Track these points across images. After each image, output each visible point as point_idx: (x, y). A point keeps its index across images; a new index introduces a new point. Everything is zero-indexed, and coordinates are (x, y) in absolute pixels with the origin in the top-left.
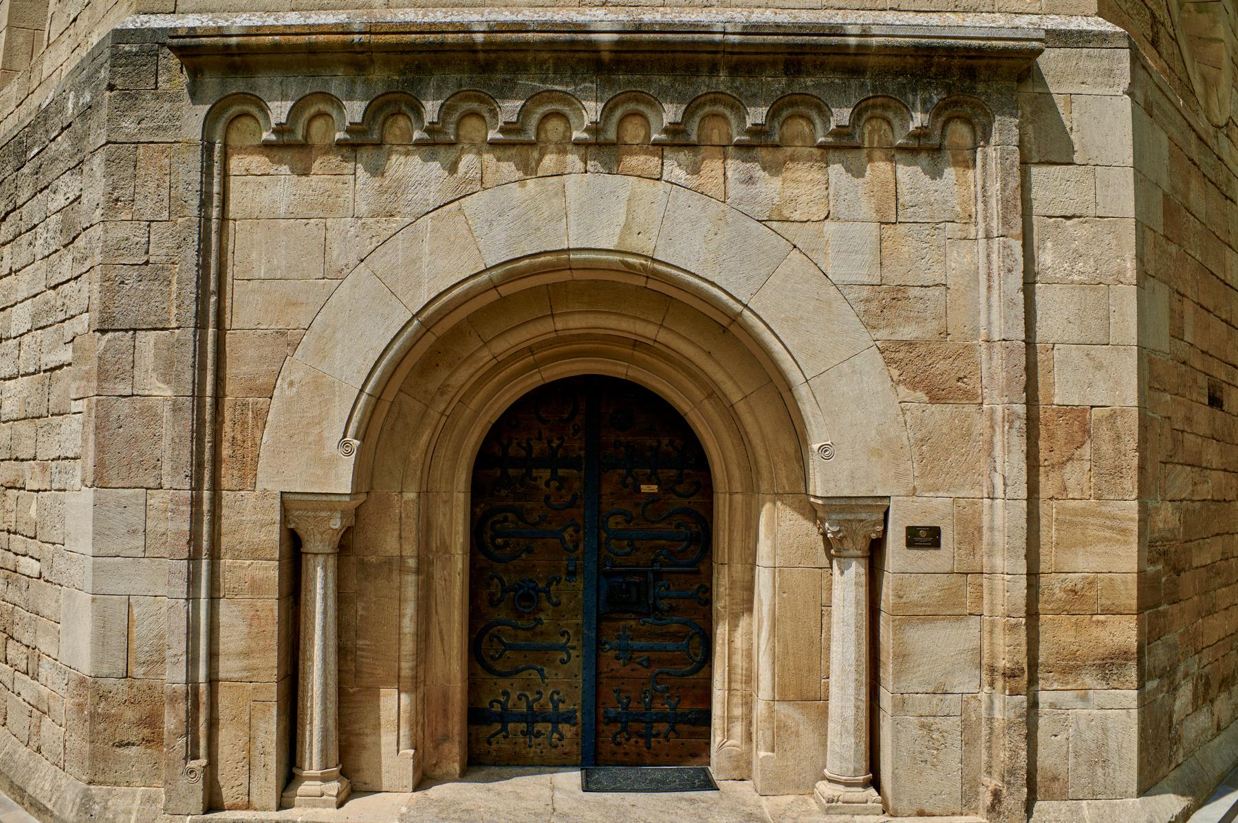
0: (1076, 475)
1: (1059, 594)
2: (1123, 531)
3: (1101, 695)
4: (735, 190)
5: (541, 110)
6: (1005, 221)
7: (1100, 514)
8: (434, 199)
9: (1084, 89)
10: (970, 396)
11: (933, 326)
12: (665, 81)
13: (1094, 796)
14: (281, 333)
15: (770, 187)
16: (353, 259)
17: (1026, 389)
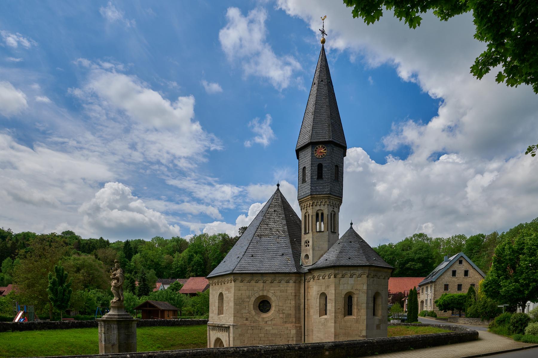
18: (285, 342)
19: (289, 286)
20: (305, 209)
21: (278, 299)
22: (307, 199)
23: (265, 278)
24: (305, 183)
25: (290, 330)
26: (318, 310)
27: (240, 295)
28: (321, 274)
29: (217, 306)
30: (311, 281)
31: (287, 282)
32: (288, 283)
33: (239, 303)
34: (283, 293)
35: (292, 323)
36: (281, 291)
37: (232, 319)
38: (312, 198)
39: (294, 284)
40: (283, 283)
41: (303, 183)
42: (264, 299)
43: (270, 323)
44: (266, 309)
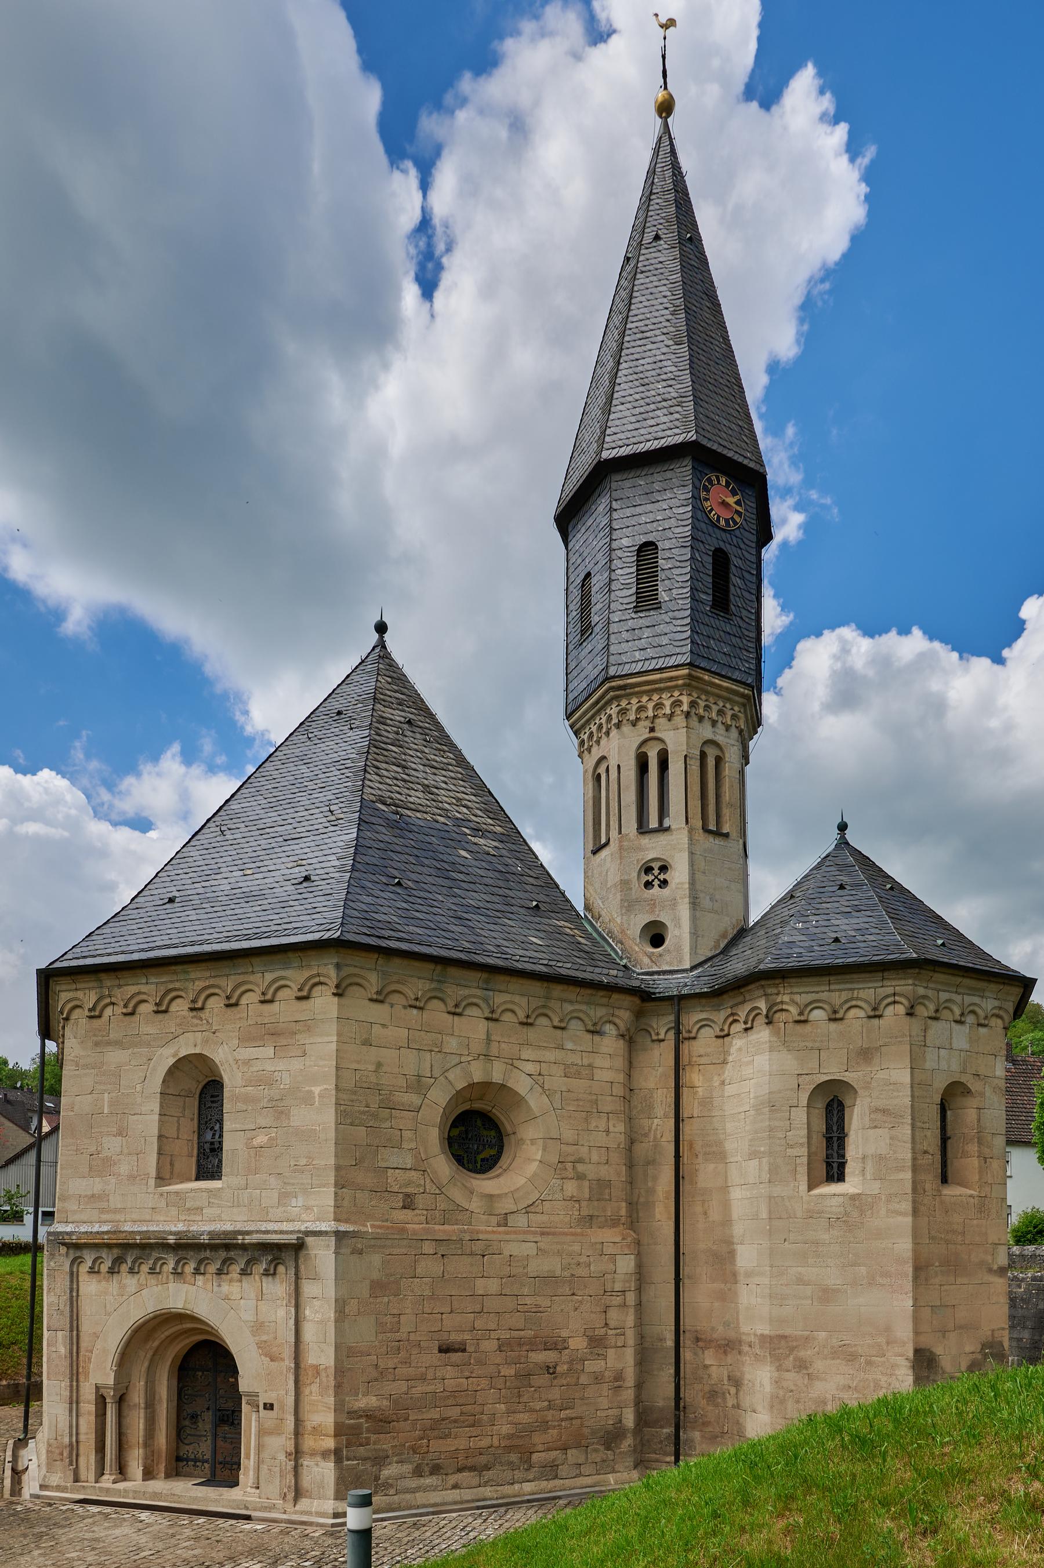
0: (315, 1388)
1: (310, 1429)
2: (329, 1408)
3: (322, 1464)
4: (216, 1289)
5: (160, 1262)
6: (289, 1302)
7: (322, 1402)
8: (134, 1290)
9: (320, 1252)
10: (283, 1360)
11: (272, 1336)
12: (192, 1253)
13: (320, 1498)
14: (95, 1333)
15: (225, 1288)
16: (113, 1310)
17: (295, 1358)
18: (593, 1315)
19: (604, 1050)
20: (644, 724)
21: (557, 1105)
22: (661, 681)
23: (499, 999)
24: (652, 613)
25: (613, 1258)
26: (805, 1160)
27: (372, 1068)
28: (824, 996)
29: (156, 1132)
30: (699, 1036)
31: (592, 1032)
32: (597, 1038)
33: (364, 1113)
34: (574, 1082)
35: (614, 1223)
36: (570, 1072)
37: (326, 1198)
38: (692, 684)
39: (621, 1042)
40: (578, 1033)
41: (637, 609)
42: (477, 1106)
43: (521, 1221)
44: (482, 1156)
